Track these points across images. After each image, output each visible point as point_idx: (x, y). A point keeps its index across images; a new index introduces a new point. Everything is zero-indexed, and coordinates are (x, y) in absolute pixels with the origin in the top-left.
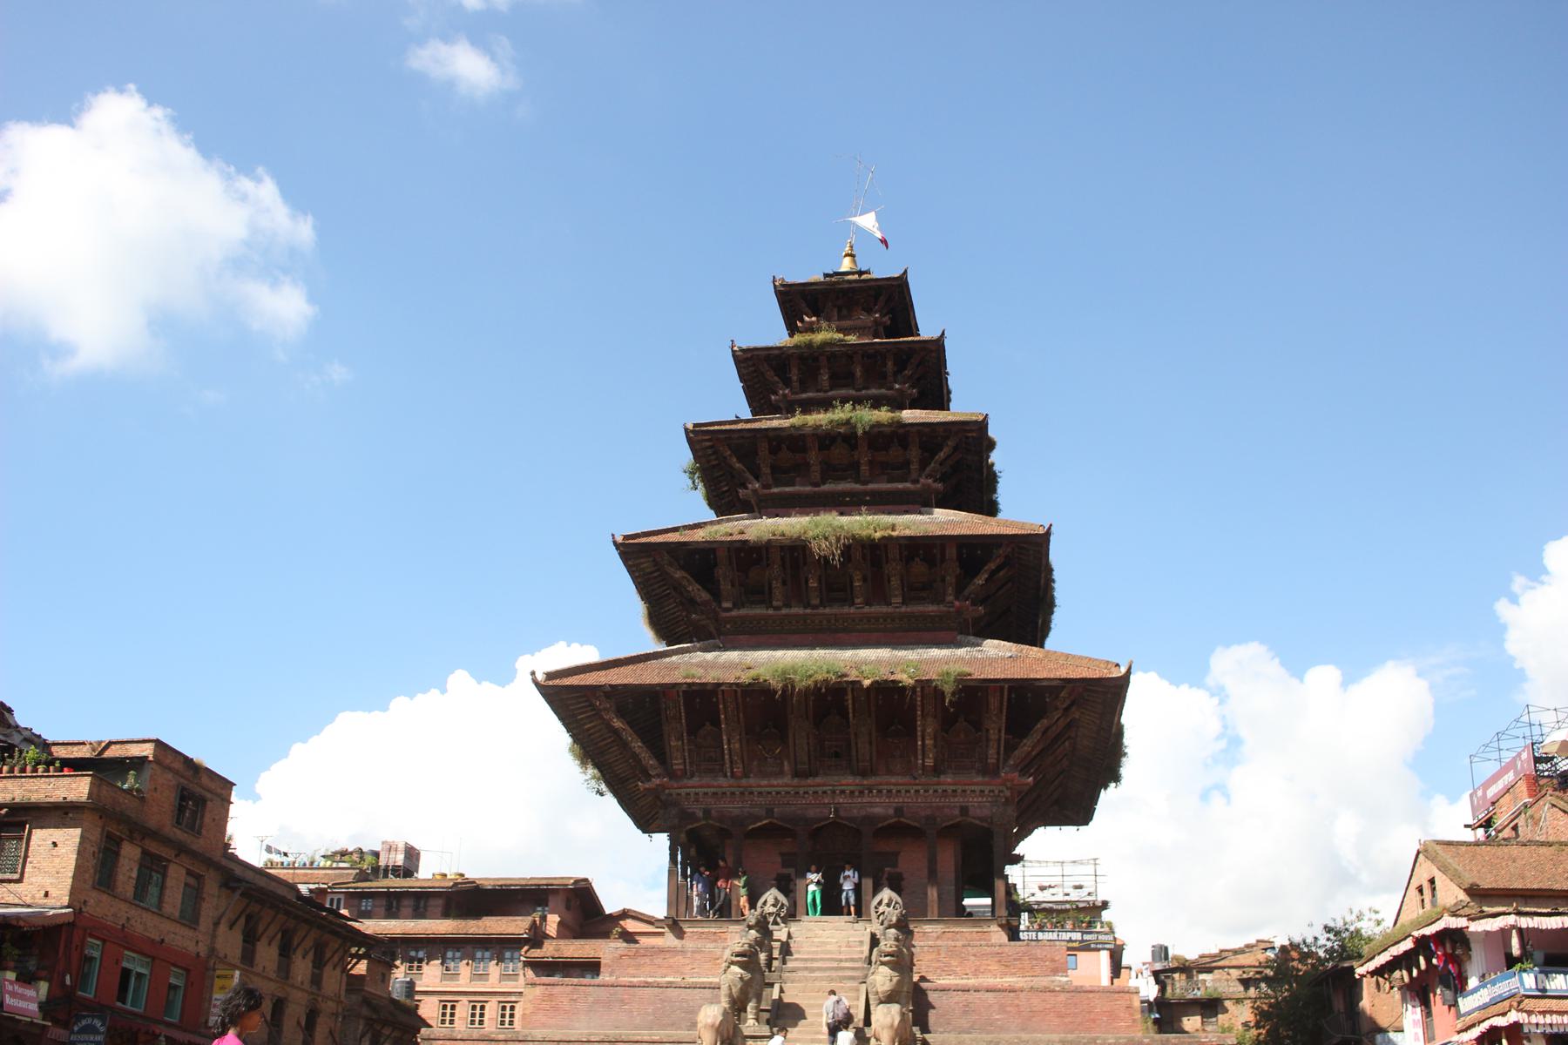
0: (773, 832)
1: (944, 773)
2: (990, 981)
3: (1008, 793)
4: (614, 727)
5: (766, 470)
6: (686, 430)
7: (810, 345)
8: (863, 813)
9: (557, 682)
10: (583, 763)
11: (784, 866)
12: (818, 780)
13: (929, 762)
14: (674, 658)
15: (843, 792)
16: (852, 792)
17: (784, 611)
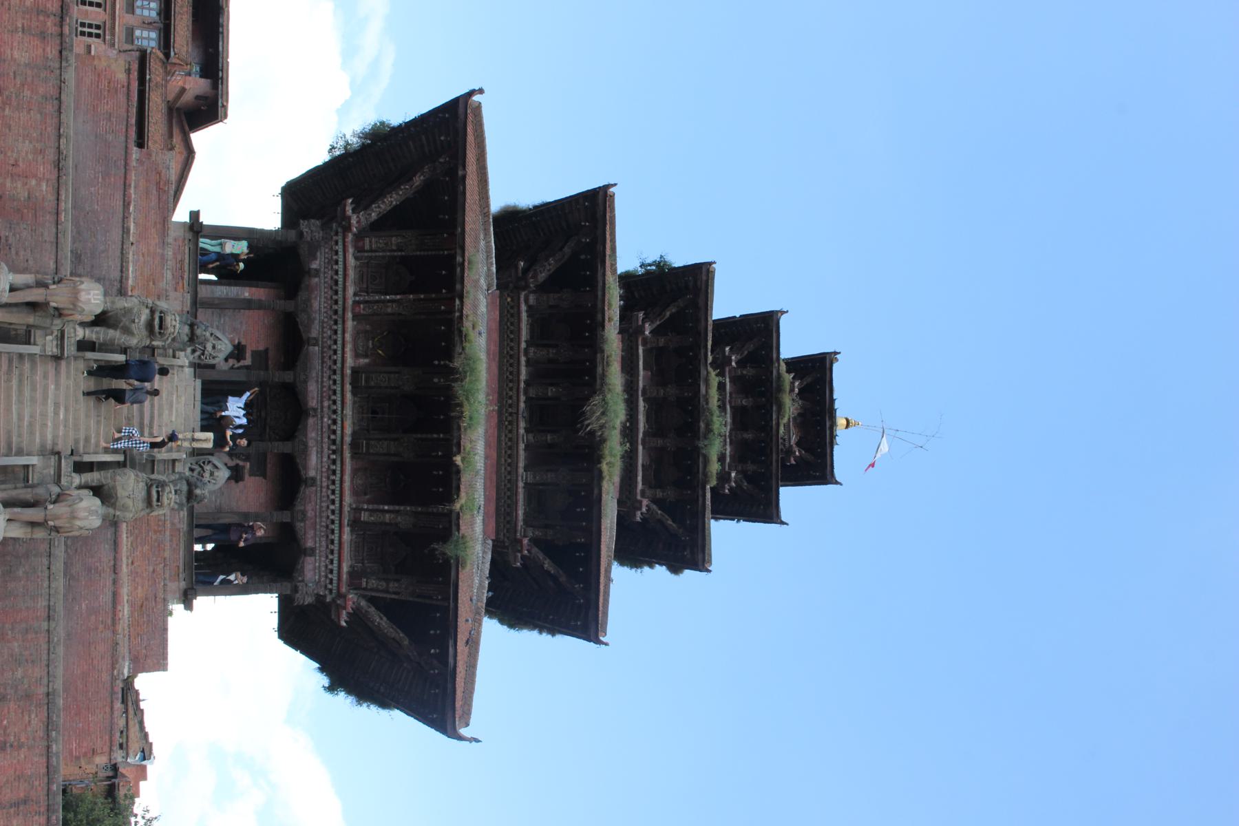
0: (291, 340)
1: (352, 531)
2: (125, 591)
4: (407, 176)
5: (662, 342)
6: (710, 264)
7: (780, 389)
8: (311, 443)
9: (470, 118)
10: (364, 135)
11: (255, 354)
12: (349, 396)
13: (364, 517)
14: (482, 243)
15: (335, 422)
16: (334, 432)
17: (523, 359)
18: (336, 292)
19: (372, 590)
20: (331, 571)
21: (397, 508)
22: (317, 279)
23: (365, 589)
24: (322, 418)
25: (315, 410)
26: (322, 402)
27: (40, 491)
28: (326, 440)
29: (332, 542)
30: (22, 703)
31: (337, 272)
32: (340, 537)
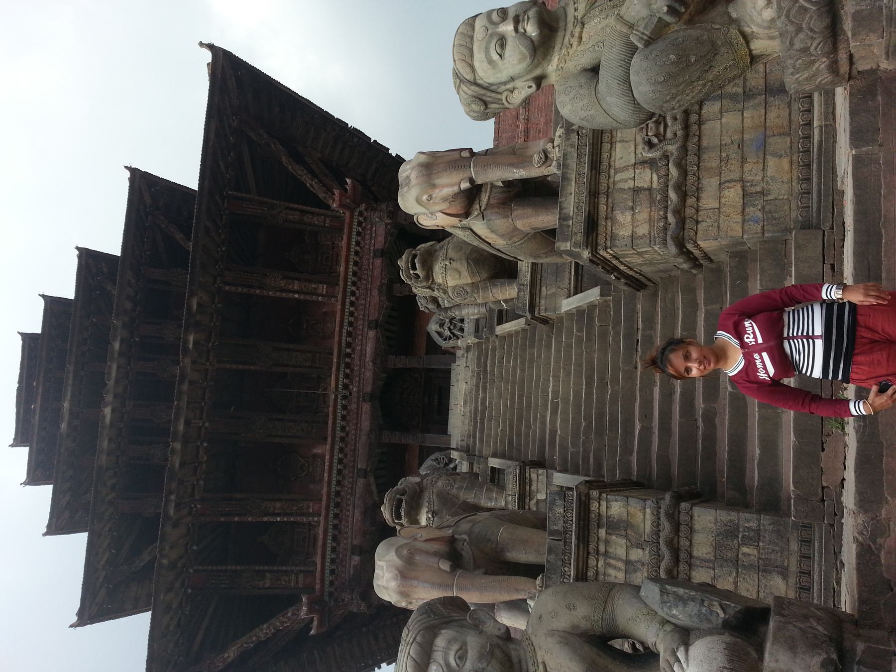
3: (363, 206)
13: (323, 288)
15: (346, 387)
16: (347, 376)
18: (335, 527)
19: (319, 215)
20: (359, 234)
21: (284, 295)
22: (355, 543)
23: (326, 216)
24: (359, 391)
25: (364, 400)
26: (358, 409)
27: (501, 223)
28: (356, 368)
29: (356, 263)
31: (334, 550)
32: (347, 268)
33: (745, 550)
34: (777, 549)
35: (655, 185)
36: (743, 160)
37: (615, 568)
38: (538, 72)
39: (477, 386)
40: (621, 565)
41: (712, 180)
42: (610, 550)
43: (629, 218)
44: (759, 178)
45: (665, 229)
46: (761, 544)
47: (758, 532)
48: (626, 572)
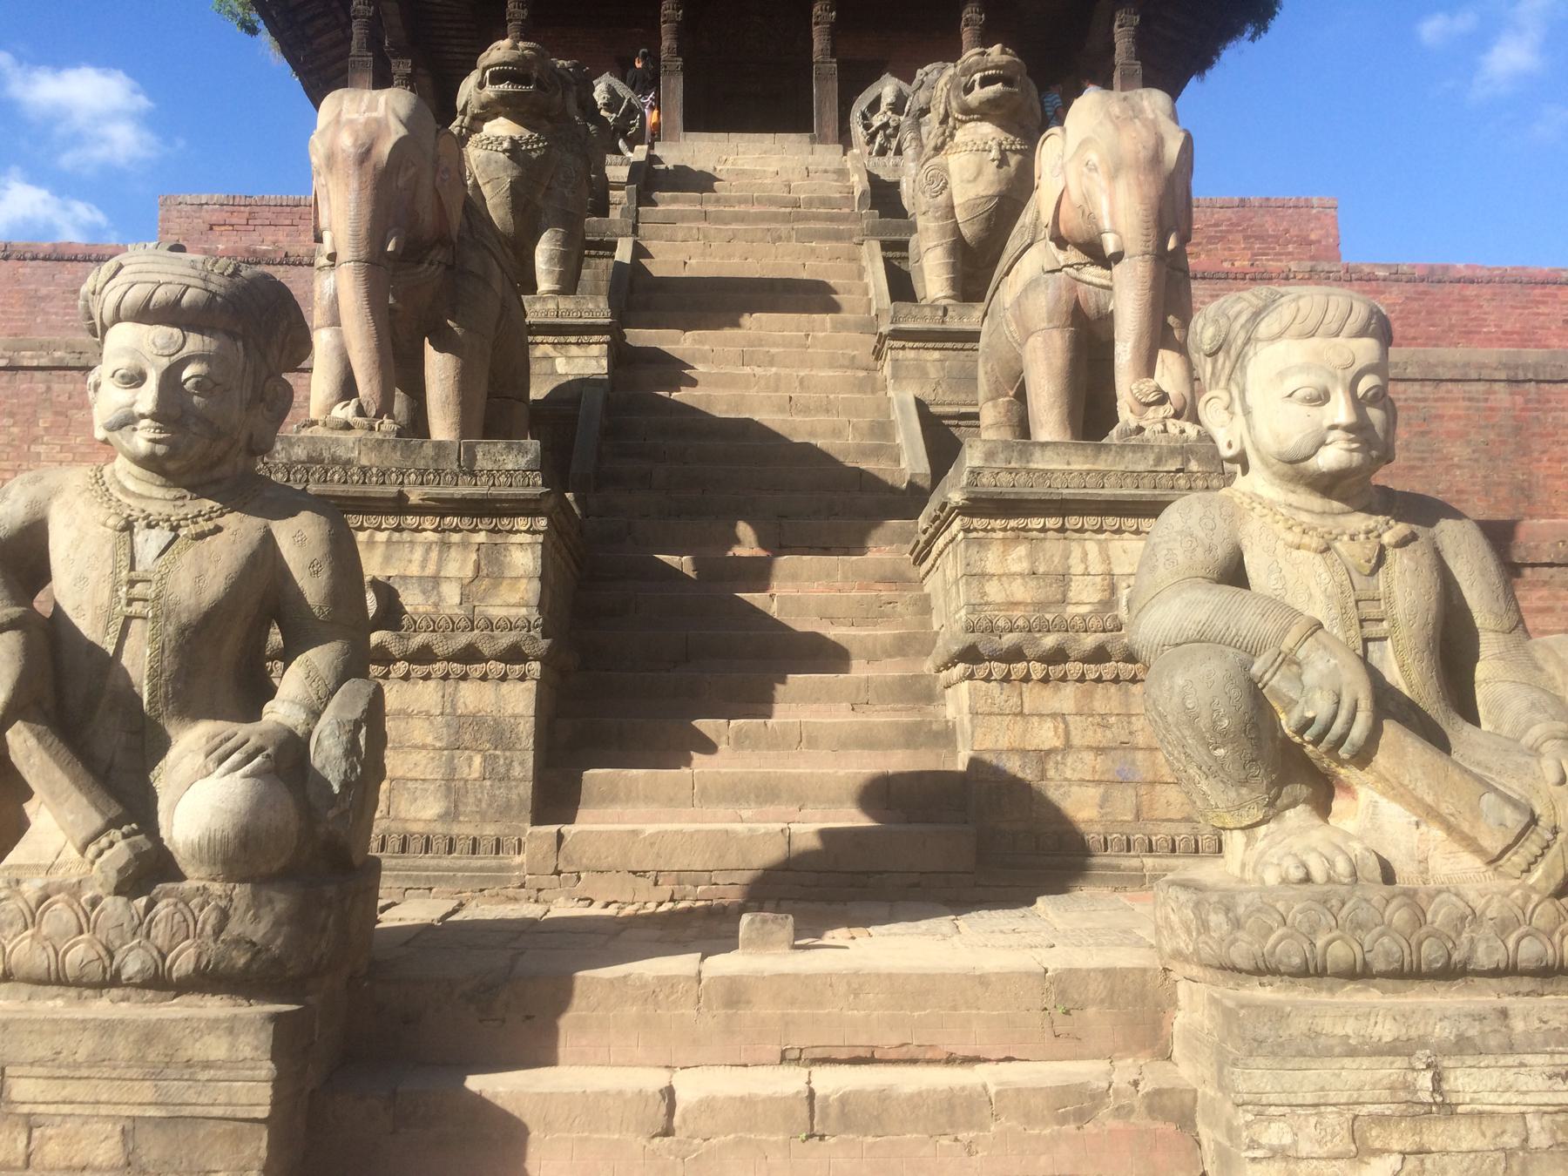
27: (1042, 305)
30: (1537, 445)
33: (477, 760)
34: (484, 805)
35: (1071, 610)
36: (1099, 750)
37: (425, 561)
38: (1253, 460)
39: (772, 201)
40: (431, 570)
41: (1072, 702)
42: (454, 553)
43: (1016, 568)
44: (1069, 774)
45: (992, 630)
46: (488, 783)
47: (505, 778)
48: (420, 578)
